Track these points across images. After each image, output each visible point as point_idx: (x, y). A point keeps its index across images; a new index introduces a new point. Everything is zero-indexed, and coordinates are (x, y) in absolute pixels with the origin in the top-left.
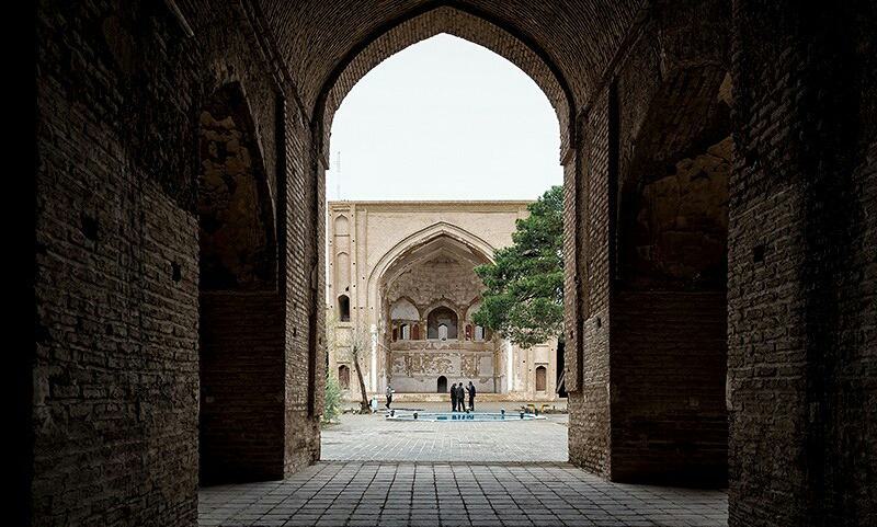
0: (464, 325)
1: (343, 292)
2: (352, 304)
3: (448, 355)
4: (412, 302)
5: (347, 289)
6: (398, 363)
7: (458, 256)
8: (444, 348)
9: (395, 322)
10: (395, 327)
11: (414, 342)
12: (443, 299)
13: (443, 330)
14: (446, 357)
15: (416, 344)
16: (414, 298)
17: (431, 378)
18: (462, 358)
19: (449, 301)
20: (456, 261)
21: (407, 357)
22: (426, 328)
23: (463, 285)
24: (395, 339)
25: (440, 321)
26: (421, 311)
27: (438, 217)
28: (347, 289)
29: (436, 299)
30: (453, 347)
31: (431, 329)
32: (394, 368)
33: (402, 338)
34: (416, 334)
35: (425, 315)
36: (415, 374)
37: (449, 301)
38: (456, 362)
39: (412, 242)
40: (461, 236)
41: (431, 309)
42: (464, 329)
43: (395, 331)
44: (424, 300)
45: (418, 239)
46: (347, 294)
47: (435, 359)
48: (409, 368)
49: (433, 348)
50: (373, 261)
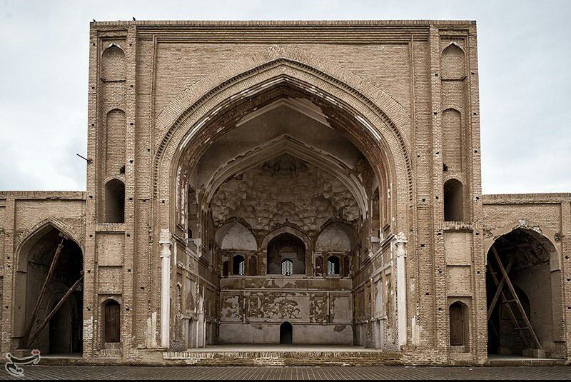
0: (314, 257)
3: (293, 294)
4: (247, 226)
6: (230, 305)
8: (289, 286)
9: (227, 252)
10: (225, 259)
11: (249, 278)
13: (287, 267)
14: (290, 298)
16: (251, 222)
17: (270, 324)
18: (312, 299)
19: (294, 226)
21: (241, 297)
22: (265, 260)
24: (226, 274)
25: (285, 255)
26: (259, 239)
30: (300, 285)
31: (273, 265)
32: (224, 311)
33: (236, 272)
34: (253, 269)
35: (265, 244)
36: (251, 319)
37: (294, 226)
38: (304, 304)
39: (231, 92)
41: (271, 237)
42: (314, 262)
43: (226, 264)
45: (243, 88)
47: (277, 300)
48: (244, 311)
49: (274, 286)
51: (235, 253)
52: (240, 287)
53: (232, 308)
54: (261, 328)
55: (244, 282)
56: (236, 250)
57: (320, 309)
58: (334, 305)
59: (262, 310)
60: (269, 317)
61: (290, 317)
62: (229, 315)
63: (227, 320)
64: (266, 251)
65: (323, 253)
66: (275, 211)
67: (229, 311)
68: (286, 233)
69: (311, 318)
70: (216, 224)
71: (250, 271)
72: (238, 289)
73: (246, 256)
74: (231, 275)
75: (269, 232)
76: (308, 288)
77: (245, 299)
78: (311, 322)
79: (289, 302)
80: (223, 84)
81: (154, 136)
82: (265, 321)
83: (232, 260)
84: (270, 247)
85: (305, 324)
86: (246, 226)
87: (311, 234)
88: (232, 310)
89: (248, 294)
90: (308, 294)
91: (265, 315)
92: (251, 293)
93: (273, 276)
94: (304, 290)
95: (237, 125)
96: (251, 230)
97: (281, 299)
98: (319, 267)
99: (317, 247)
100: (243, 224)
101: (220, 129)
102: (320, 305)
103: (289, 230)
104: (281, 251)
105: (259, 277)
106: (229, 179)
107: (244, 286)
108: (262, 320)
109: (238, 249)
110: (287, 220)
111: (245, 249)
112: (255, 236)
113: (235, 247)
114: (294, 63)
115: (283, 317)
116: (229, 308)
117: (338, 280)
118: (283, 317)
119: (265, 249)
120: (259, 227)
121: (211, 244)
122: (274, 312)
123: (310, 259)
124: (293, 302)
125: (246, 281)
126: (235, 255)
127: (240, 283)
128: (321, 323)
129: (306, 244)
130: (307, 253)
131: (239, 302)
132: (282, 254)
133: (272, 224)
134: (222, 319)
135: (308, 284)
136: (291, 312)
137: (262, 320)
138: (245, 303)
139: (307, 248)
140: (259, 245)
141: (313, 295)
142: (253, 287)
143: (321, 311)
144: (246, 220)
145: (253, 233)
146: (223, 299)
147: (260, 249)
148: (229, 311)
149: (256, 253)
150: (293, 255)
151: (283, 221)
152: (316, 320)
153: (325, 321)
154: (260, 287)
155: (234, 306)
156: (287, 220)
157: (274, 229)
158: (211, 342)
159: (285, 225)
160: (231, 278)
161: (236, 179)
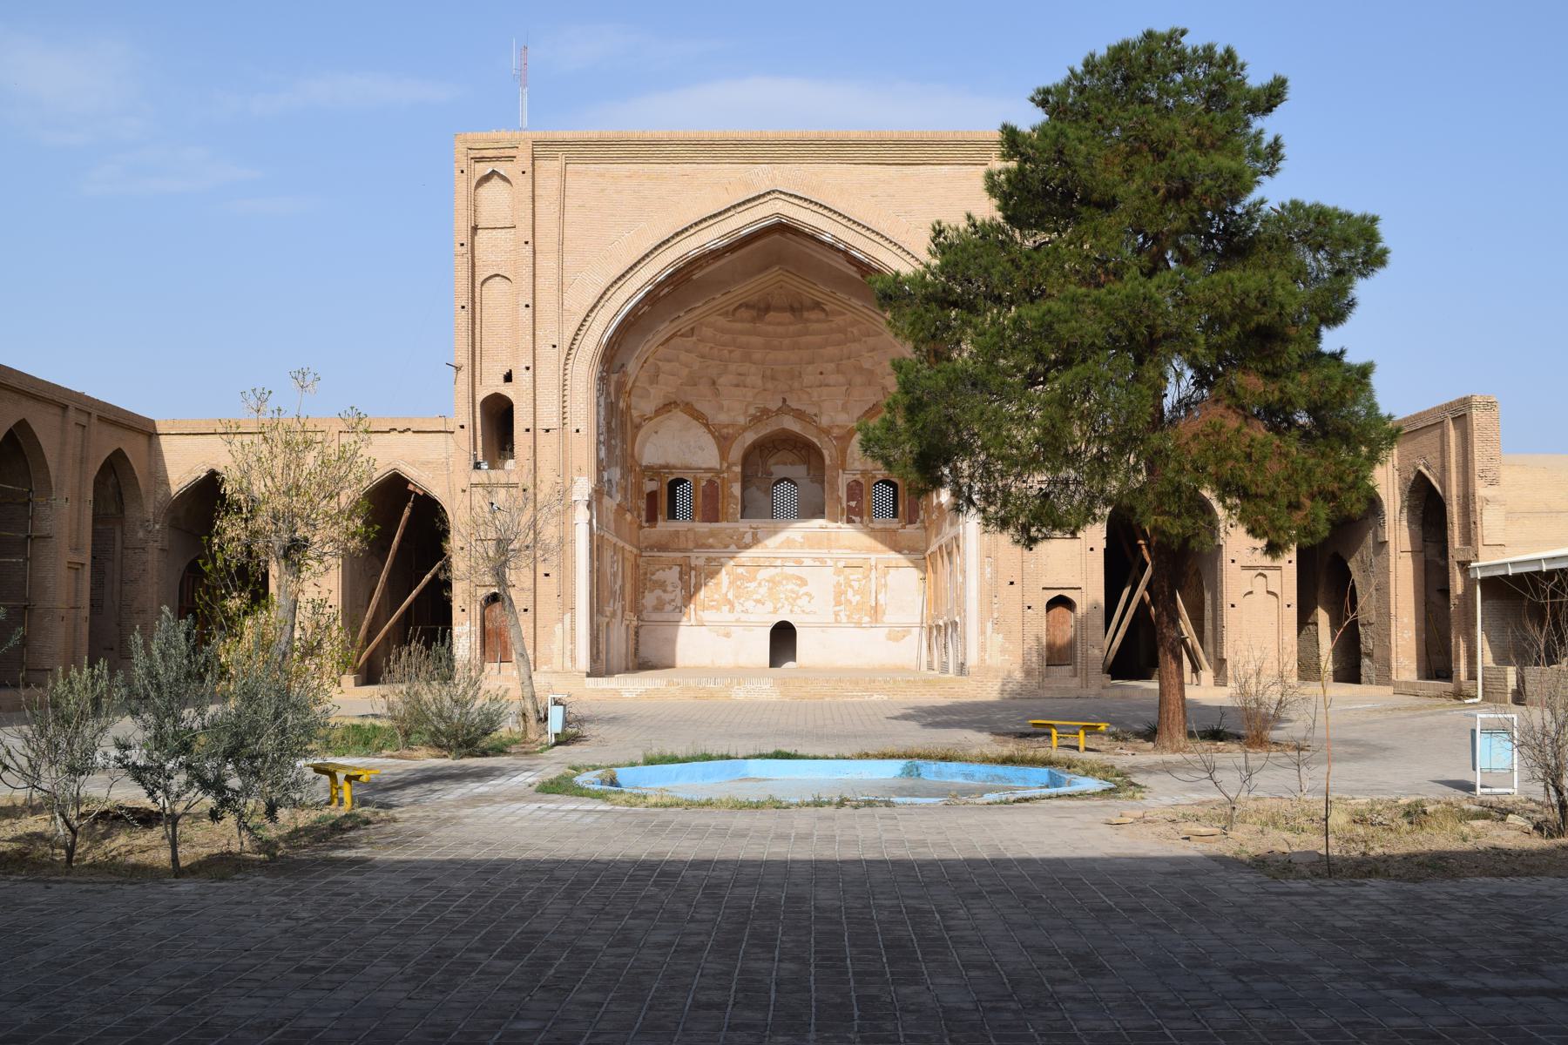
0: (843, 480)
1: (491, 384)
2: (521, 420)
4: (698, 416)
5: (508, 378)
6: (662, 585)
7: (819, 292)
9: (654, 472)
10: (650, 486)
11: (703, 527)
12: (785, 409)
15: (712, 534)
16: (704, 407)
18: (838, 572)
19: (799, 415)
20: (817, 306)
22: (736, 489)
23: (838, 371)
24: (652, 518)
25: (779, 471)
26: (723, 441)
27: (763, 176)
28: (508, 378)
29: (765, 412)
31: (754, 492)
32: (650, 599)
35: (736, 453)
36: (707, 616)
37: (799, 415)
38: (822, 582)
40: (830, 229)
41: (750, 438)
42: (843, 493)
43: (652, 497)
44: (733, 411)
45: (710, 237)
46: (507, 390)
50: (580, 301)
51: (672, 474)
52: (681, 546)
53: (665, 591)
54: (728, 635)
55: (691, 536)
56: (674, 467)
57: (856, 592)
58: (885, 585)
59: (730, 596)
60: (746, 611)
61: (791, 611)
62: (659, 608)
63: (656, 616)
64: (738, 469)
65: (864, 473)
66: (759, 382)
67: (659, 598)
68: (783, 429)
69: (836, 614)
70: (637, 420)
71: (703, 515)
72: (680, 550)
73: (695, 478)
74: (664, 520)
75: (745, 429)
76: (830, 547)
77: (693, 573)
78: (836, 621)
79: (788, 578)
80: (677, 234)
81: (561, 322)
82: (738, 620)
83: (665, 488)
84: (746, 460)
85: (824, 626)
86: (697, 419)
87: (836, 432)
88: (667, 597)
89: (701, 562)
90: (829, 562)
91: (738, 607)
92: (708, 560)
93: (755, 523)
94: (822, 553)
95: (694, 277)
96: (707, 425)
97: (772, 571)
98: (853, 504)
99: (849, 460)
100: (691, 415)
101: (666, 290)
102: (856, 585)
103: (791, 425)
104: (772, 461)
105: (723, 525)
106: (668, 340)
107: (691, 545)
108: (731, 617)
109: (679, 465)
110: (784, 400)
111: (694, 464)
112: (714, 437)
113: (672, 461)
114: (796, 197)
115: (776, 610)
116: (658, 592)
117: (895, 531)
118: (776, 610)
119: (735, 464)
120: (723, 418)
121: (629, 463)
122: (758, 601)
123: (835, 488)
124: (799, 578)
125: (695, 533)
126: (671, 478)
127: (682, 539)
128: (859, 625)
129: (826, 453)
130: (827, 473)
131: (681, 578)
132: (774, 469)
133: (752, 411)
134: (645, 615)
135: (829, 539)
136: (795, 600)
137: (731, 617)
138: (693, 581)
139: (827, 461)
140: (723, 454)
141: (841, 564)
142: (711, 547)
143: (858, 598)
144: (698, 406)
145: (710, 431)
146: (646, 574)
147: (725, 465)
148: (659, 598)
149: (718, 472)
150: (799, 471)
151: (775, 405)
152: (849, 617)
153: (866, 619)
154: (727, 546)
155: (670, 588)
156: (784, 400)
157: (756, 420)
158: (630, 665)
159: (779, 411)
160: (664, 526)
161: (682, 335)
